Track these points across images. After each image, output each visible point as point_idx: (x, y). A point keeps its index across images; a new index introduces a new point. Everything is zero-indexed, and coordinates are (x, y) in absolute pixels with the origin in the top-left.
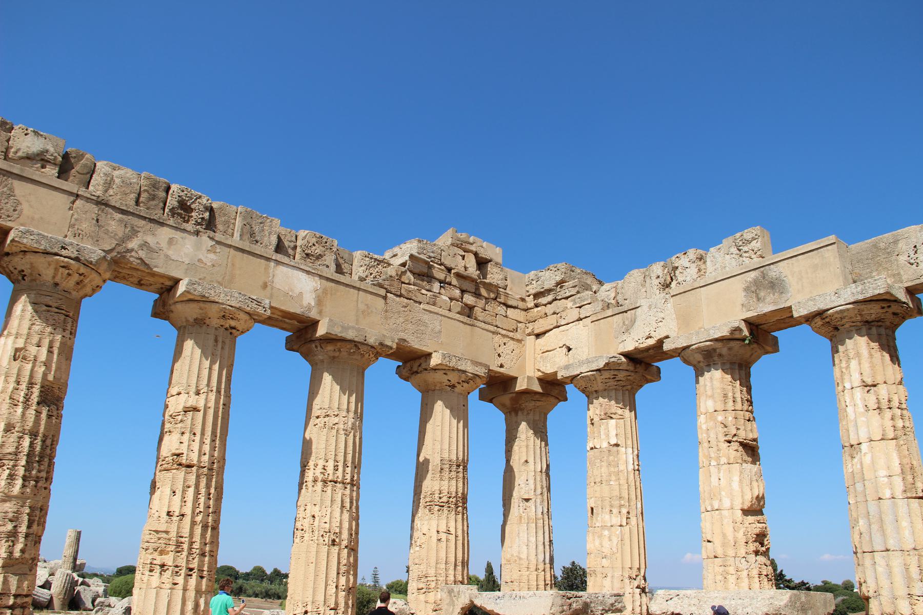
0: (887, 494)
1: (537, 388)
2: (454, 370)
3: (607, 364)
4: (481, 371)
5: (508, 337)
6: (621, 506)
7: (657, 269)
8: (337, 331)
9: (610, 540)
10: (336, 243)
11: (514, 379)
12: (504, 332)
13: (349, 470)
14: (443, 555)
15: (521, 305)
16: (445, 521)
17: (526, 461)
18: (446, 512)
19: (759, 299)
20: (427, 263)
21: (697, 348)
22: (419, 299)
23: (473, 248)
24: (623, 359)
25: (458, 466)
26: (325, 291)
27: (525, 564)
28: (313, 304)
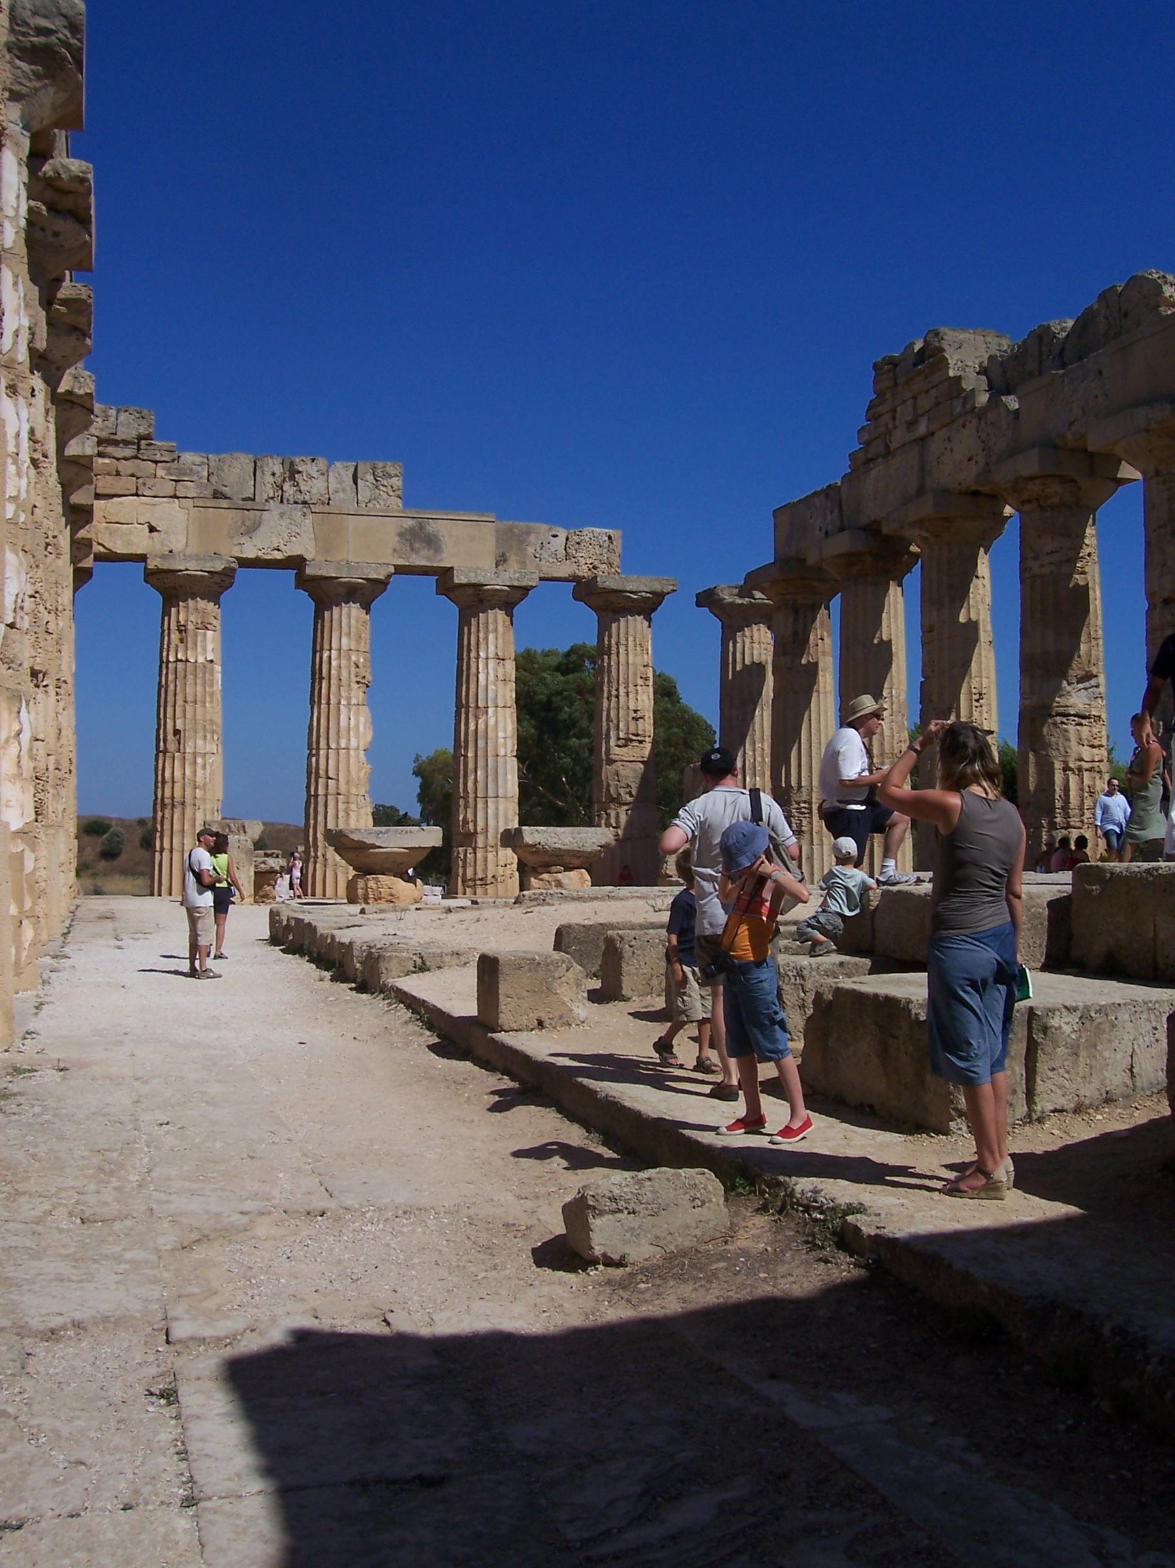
0: (502, 752)
6: (213, 732)
19: (412, 550)
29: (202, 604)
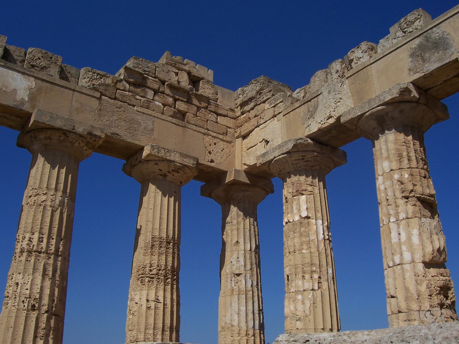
1: (244, 179)
2: (164, 160)
3: (295, 146)
4: (190, 162)
5: (217, 138)
6: (312, 272)
7: (336, 65)
8: (46, 120)
9: (303, 303)
10: (60, 59)
11: (224, 174)
12: (214, 134)
13: (53, 242)
14: (151, 321)
15: (230, 114)
16: (154, 291)
17: (237, 242)
18: (155, 282)
19: (424, 61)
20: (141, 74)
21: (370, 115)
22: (134, 102)
23: (187, 68)
24: (310, 141)
25: (169, 243)
26: (39, 90)
27: (236, 329)
28: (27, 99)
29: (294, 179)
